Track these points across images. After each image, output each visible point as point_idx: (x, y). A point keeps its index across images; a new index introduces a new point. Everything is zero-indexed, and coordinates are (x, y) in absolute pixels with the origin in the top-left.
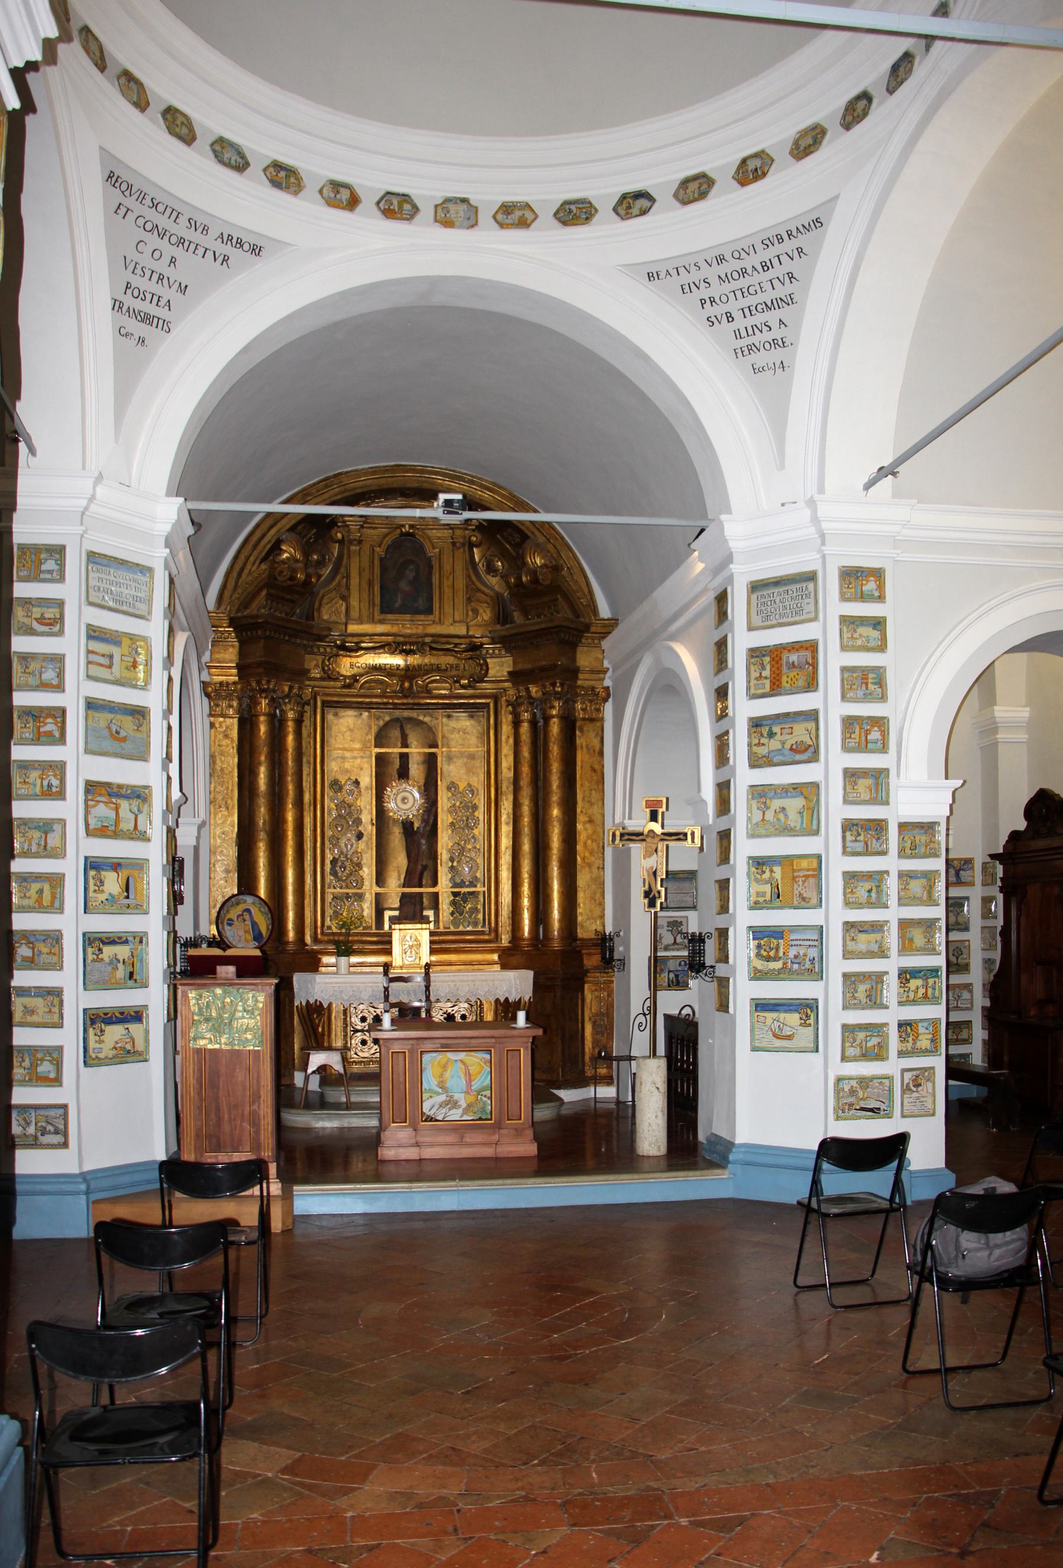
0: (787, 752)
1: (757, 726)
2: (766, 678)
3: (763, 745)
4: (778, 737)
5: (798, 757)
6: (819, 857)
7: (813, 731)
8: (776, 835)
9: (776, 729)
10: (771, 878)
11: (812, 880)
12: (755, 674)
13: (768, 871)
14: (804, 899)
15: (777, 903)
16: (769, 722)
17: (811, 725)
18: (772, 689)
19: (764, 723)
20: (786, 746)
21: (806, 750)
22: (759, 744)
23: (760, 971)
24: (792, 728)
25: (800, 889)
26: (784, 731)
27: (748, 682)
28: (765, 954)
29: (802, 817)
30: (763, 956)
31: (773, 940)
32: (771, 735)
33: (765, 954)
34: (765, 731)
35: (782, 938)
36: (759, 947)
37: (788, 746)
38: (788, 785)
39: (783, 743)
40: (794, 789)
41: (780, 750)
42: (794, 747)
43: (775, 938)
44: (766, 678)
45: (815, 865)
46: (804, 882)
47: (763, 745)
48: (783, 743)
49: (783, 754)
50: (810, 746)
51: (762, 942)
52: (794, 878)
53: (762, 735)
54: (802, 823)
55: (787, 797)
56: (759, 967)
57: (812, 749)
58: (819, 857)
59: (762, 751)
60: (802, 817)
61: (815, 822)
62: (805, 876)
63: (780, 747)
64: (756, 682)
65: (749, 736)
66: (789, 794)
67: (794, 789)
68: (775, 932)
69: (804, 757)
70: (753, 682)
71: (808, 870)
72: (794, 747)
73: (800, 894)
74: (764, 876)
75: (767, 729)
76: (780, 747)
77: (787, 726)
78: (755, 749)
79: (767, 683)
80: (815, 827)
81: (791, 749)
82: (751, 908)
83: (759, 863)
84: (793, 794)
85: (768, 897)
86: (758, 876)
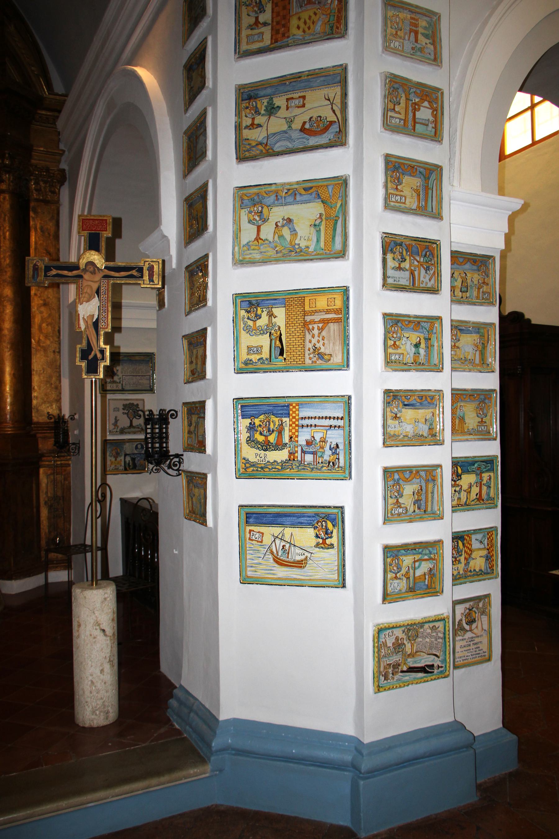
0: (295, 135)
1: (250, 98)
2: (265, 24)
3: (259, 126)
4: (283, 113)
5: (313, 141)
6: (345, 291)
7: (338, 100)
8: (277, 261)
9: (279, 101)
10: (270, 324)
11: (333, 327)
12: (247, 20)
13: (264, 315)
14: (321, 356)
15: (279, 362)
16: (269, 91)
17: (335, 92)
18: (274, 39)
19: (262, 93)
20: (294, 126)
21: (326, 129)
22: (253, 126)
23: (253, 465)
24: (304, 97)
25: (314, 341)
26: (293, 103)
27: (238, 33)
28: (261, 439)
29: (319, 231)
30: (258, 442)
31: (273, 418)
32: (272, 110)
33: (261, 439)
34: (263, 103)
35: (288, 415)
36: (251, 428)
37: (297, 125)
38: (298, 183)
39: (290, 121)
40: (305, 189)
41: (285, 132)
42: (307, 126)
43: (276, 415)
44: (265, 24)
45: (339, 303)
46: (321, 330)
47: (259, 126)
48: (290, 121)
49: (290, 139)
50: (331, 123)
51: (257, 422)
52: (306, 324)
53: (257, 112)
54: (318, 241)
55: (295, 202)
56: (252, 459)
57: (334, 128)
58: (345, 291)
59: (257, 135)
60: (319, 231)
61: (338, 239)
62: (322, 321)
63: (285, 127)
64: (249, 32)
65: (238, 113)
66: (298, 198)
67: (305, 189)
68: (276, 406)
69: (323, 139)
70: (244, 33)
71: (328, 312)
72: (307, 126)
73: (315, 349)
74: (259, 323)
75: (265, 101)
76: (285, 127)
77: (296, 96)
78: (246, 133)
79: (267, 32)
80: (338, 246)
81: (303, 130)
82: (239, 371)
83: (250, 303)
84: (306, 197)
85: (265, 354)
86: (250, 323)
